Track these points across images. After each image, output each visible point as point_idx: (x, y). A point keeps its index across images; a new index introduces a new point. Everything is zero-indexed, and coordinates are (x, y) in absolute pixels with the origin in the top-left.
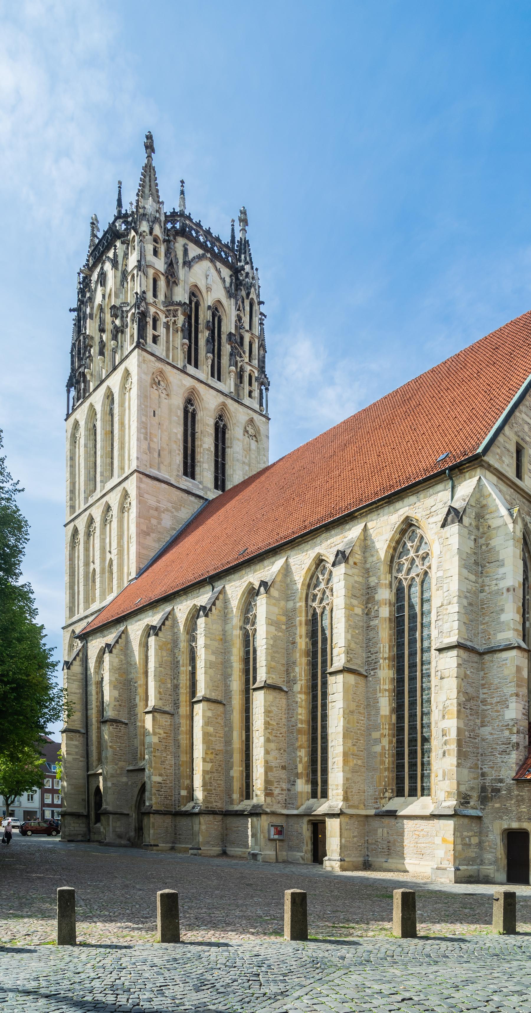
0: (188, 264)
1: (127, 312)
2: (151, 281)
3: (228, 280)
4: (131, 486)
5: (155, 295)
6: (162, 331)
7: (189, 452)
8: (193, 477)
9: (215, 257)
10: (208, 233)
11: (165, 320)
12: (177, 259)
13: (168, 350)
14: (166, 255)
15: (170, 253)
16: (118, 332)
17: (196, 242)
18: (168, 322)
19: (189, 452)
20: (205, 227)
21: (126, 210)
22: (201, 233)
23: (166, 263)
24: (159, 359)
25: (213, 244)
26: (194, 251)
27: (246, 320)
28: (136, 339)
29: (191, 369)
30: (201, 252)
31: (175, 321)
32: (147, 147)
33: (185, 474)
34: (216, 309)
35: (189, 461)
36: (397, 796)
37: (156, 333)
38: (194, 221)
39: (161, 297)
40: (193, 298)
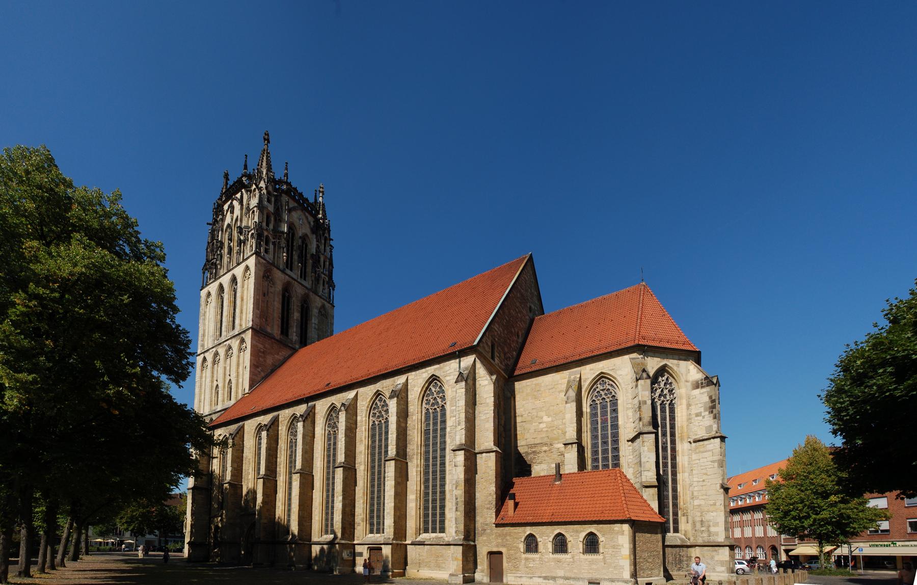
0: (290, 211)
1: (249, 232)
2: (265, 216)
3: (312, 223)
4: (248, 336)
5: (268, 225)
6: (271, 246)
7: (285, 320)
8: (287, 335)
9: (304, 209)
10: (301, 195)
11: (273, 240)
12: (282, 207)
13: (274, 258)
14: (275, 203)
15: (278, 203)
16: (241, 243)
17: (293, 199)
18: (275, 242)
19: (285, 320)
20: (299, 191)
21: (250, 172)
22: (297, 194)
23: (274, 208)
24: (268, 262)
25: (304, 202)
26: (292, 204)
27: (322, 247)
28: (254, 250)
29: (288, 272)
30: (296, 205)
31: (279, 242)
32: (265, 139)
33: (282, 333)
34: (304, 238)
35: (285, 325)
36: (424, 533)
37: (267, 247)
38: (293, 187)
39: (271, 226)
40: (290, 230)
